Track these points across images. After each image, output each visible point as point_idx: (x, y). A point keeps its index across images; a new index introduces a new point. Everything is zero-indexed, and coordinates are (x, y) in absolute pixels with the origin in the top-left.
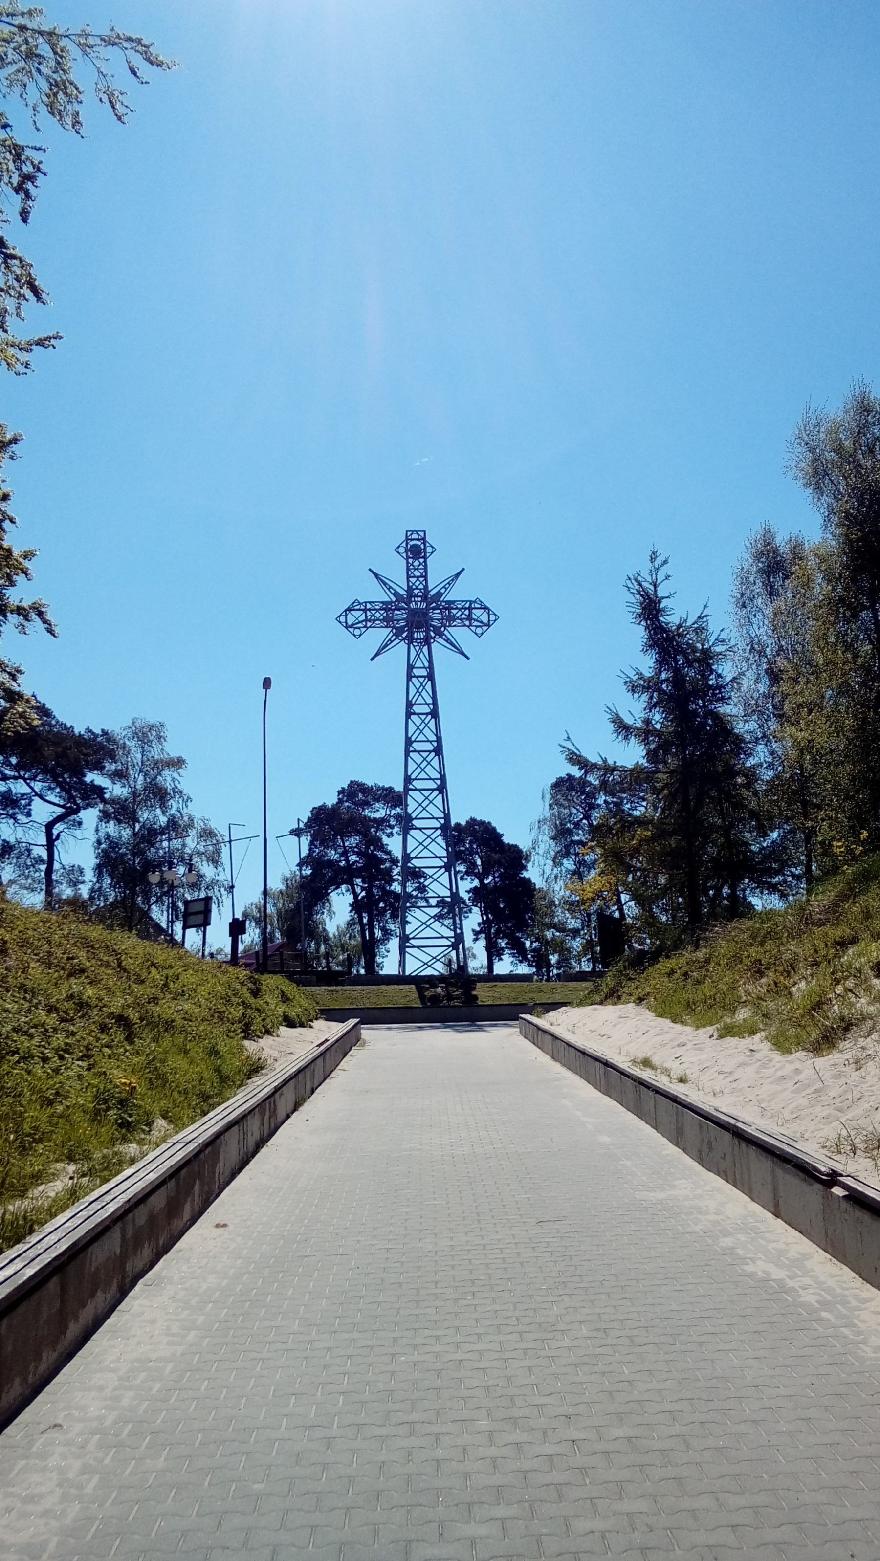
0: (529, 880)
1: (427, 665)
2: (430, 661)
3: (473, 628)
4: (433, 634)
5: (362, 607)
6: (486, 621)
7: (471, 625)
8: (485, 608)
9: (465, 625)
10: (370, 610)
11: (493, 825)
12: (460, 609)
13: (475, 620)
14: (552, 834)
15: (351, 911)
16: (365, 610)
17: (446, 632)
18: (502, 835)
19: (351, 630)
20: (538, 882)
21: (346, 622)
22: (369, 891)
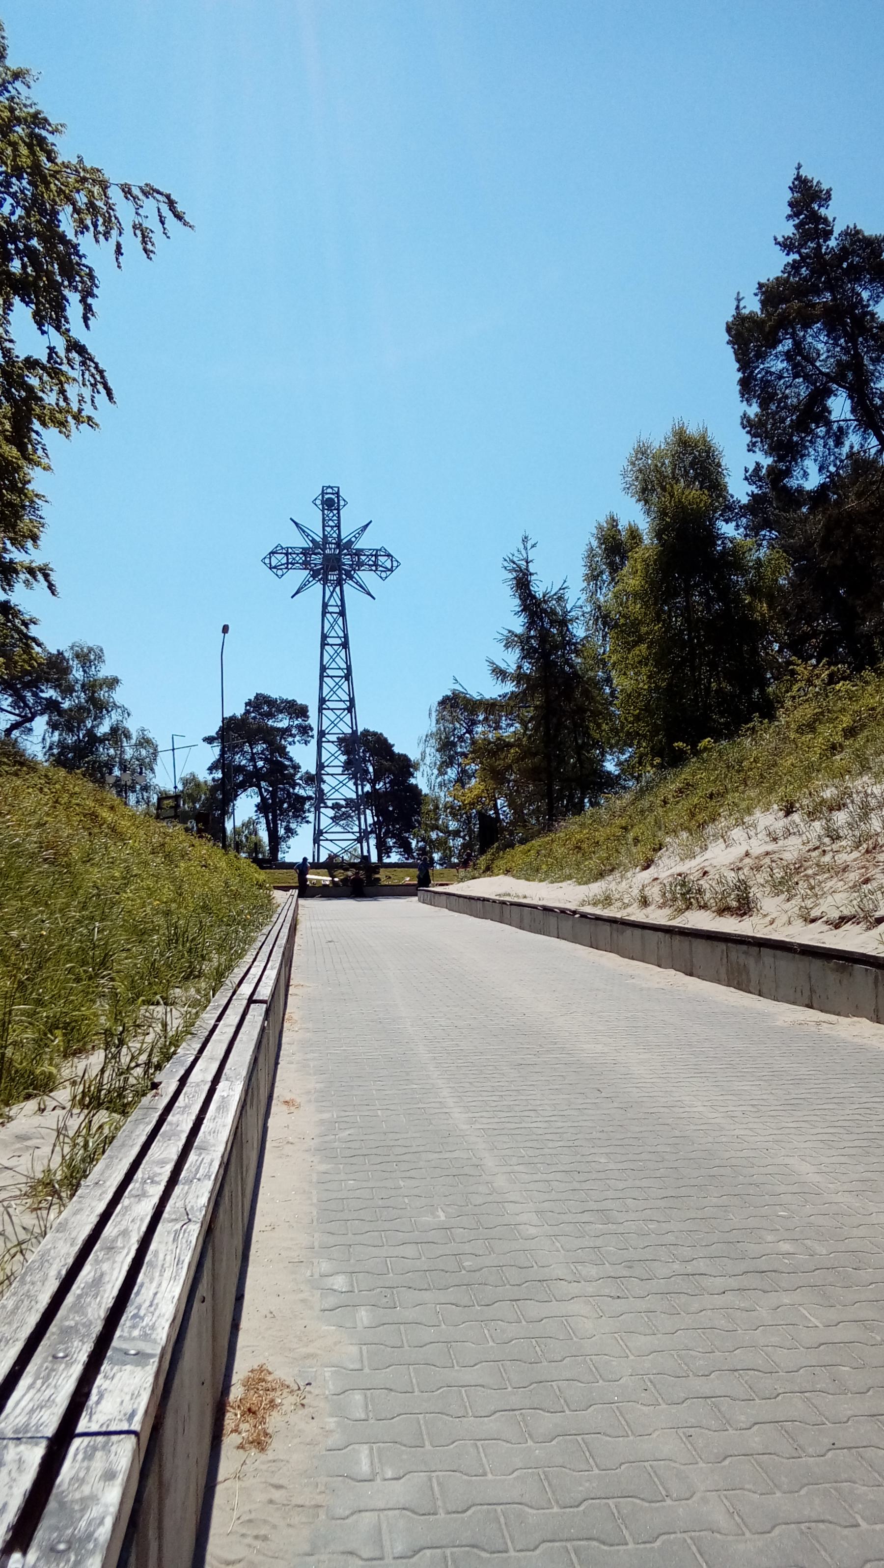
0: (416, 786)
1: (339, 603)
2: (342, 600)
3: (379, 573)
4: (344, 577)
5: (284, 551)
6: (389, 567)
7: (377, 570)
8: (389, 555)
10: (291, 554)
11: (385, 735)
12: (368, 556)
14: (438, 746)
15: (256, 811)
16: (287, 554)
17: (355, 575)
18: (393, 745)
19: (275, 570)
20: (425, 790)
22: (273, 794)
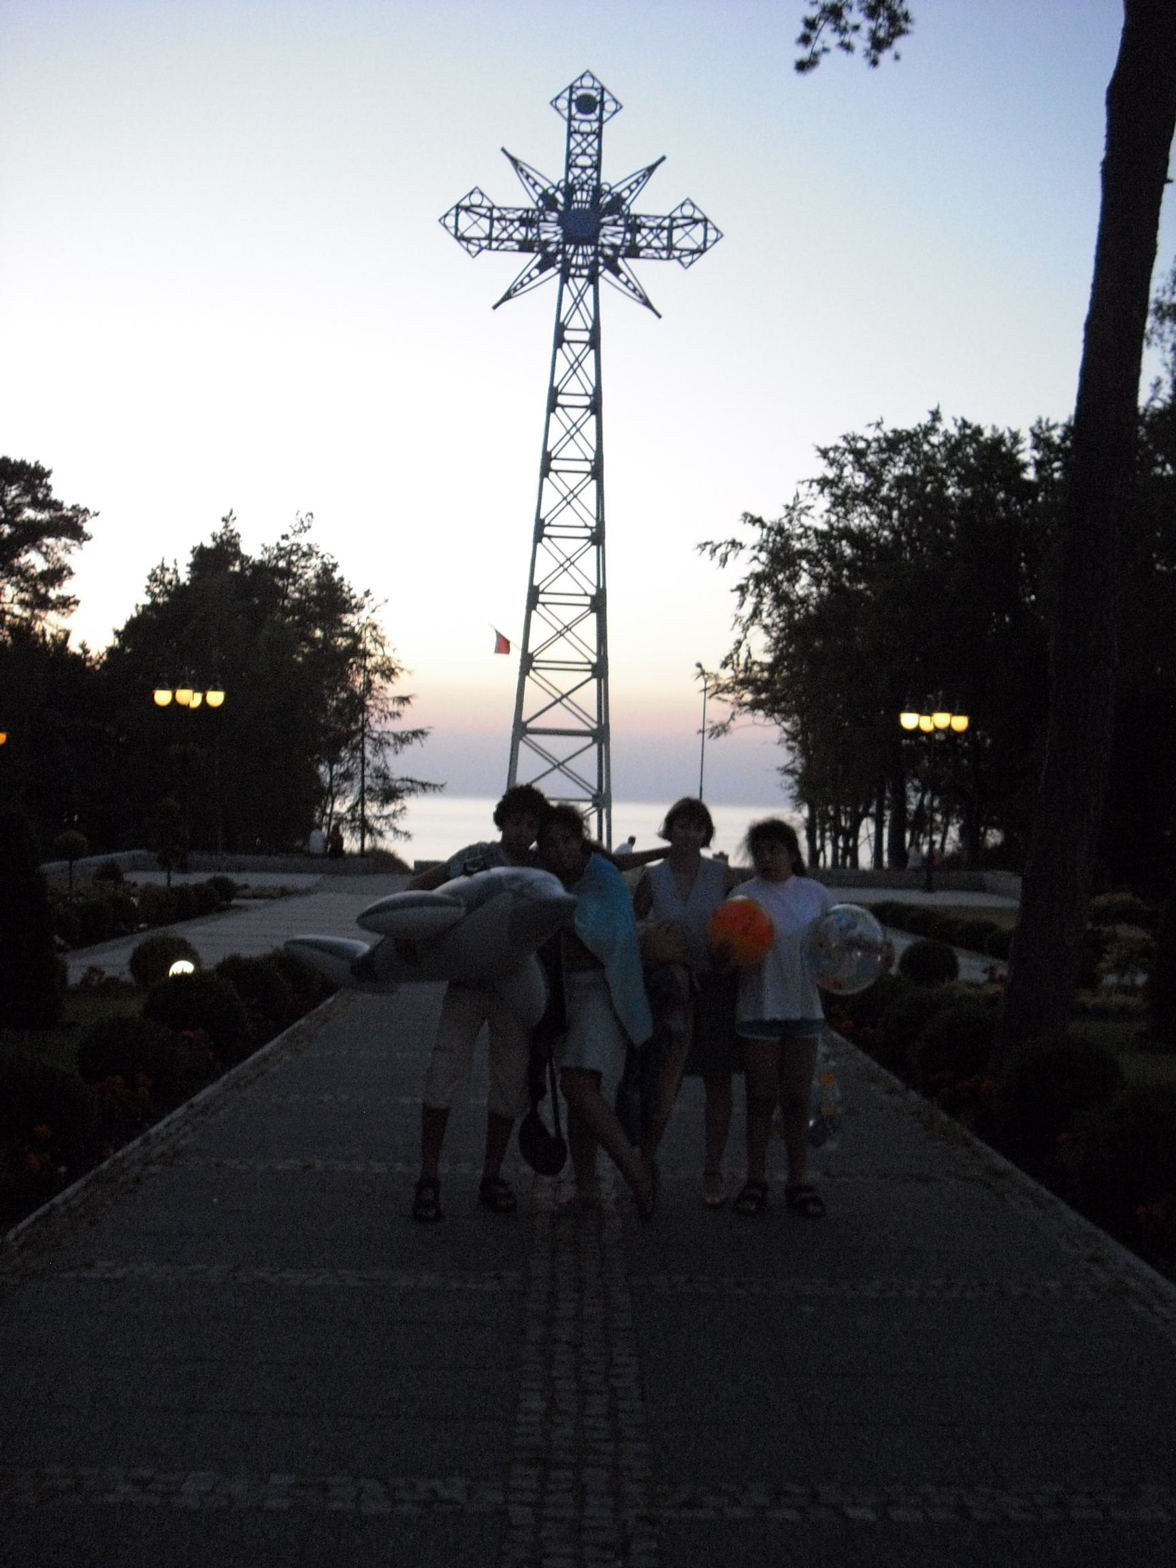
4: (560, 197)
5: (677, 253)
9: (499, 209)
10: (664, 249)
13: (481, 216)
19: (697, 215)
21: (706, 229)
